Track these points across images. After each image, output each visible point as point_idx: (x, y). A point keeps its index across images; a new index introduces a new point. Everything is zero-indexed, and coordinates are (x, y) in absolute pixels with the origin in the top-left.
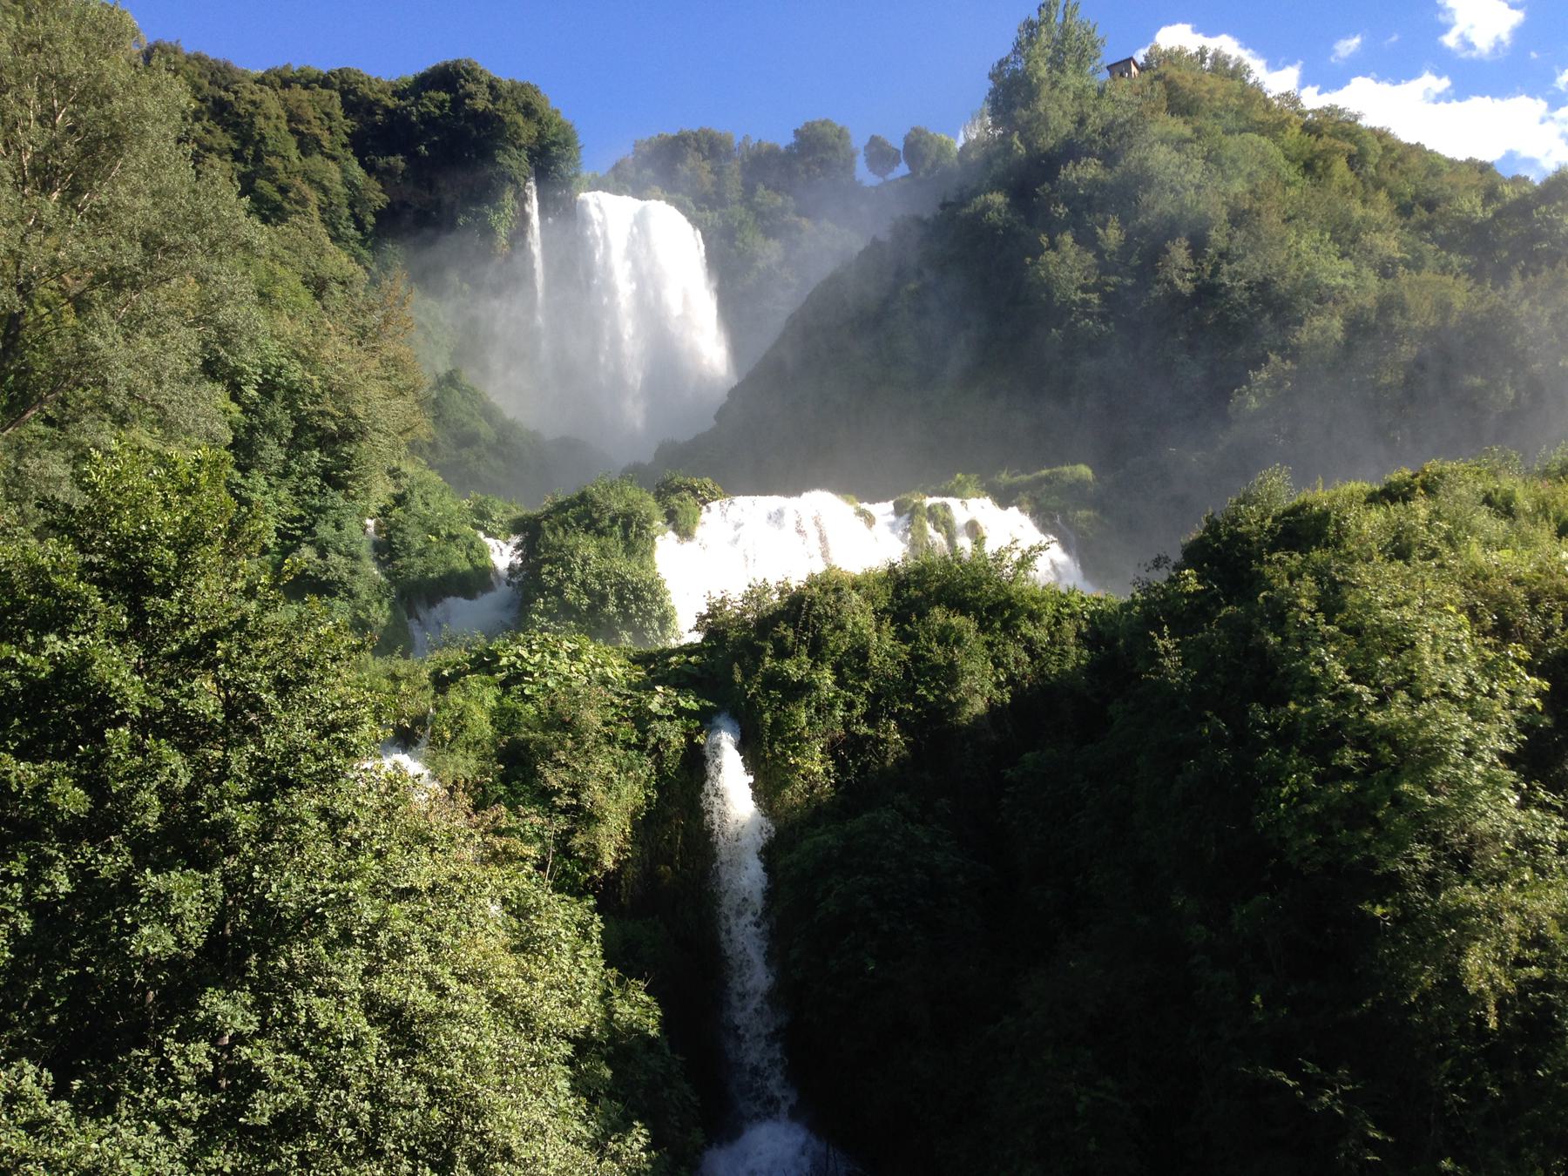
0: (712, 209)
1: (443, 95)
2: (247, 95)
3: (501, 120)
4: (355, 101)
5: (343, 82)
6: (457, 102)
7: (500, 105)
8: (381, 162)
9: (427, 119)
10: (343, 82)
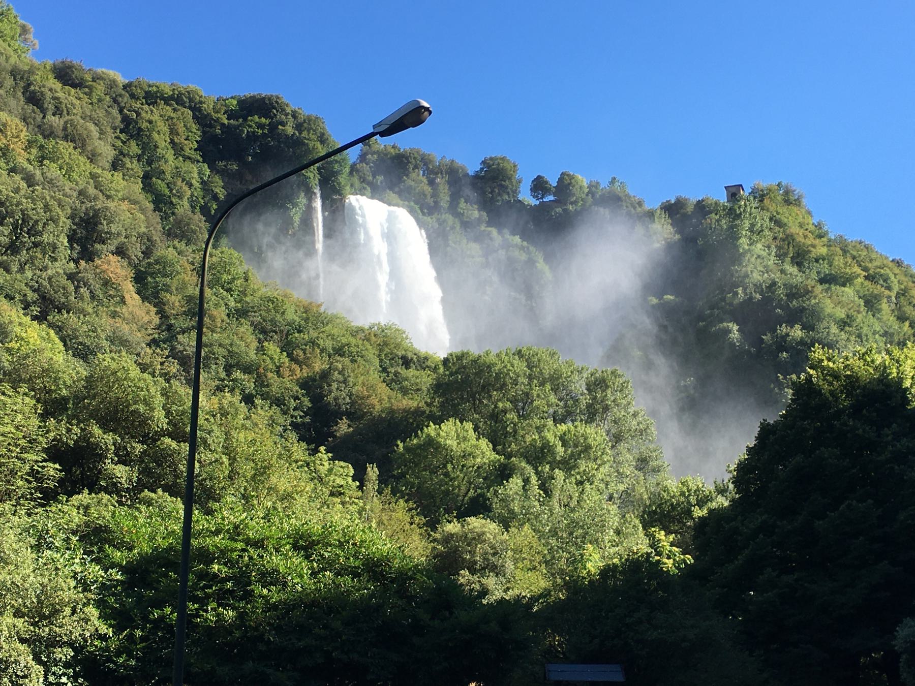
0: (430, 214)
1: (263, 120)
2: (148, 116)
3: (304, 144)
4: (202, 118)
5: (191, 100)
6: (273, 127)
7: (304, 134)
8: (221, 164)
9: (252, 137)
10: (191, 100)
